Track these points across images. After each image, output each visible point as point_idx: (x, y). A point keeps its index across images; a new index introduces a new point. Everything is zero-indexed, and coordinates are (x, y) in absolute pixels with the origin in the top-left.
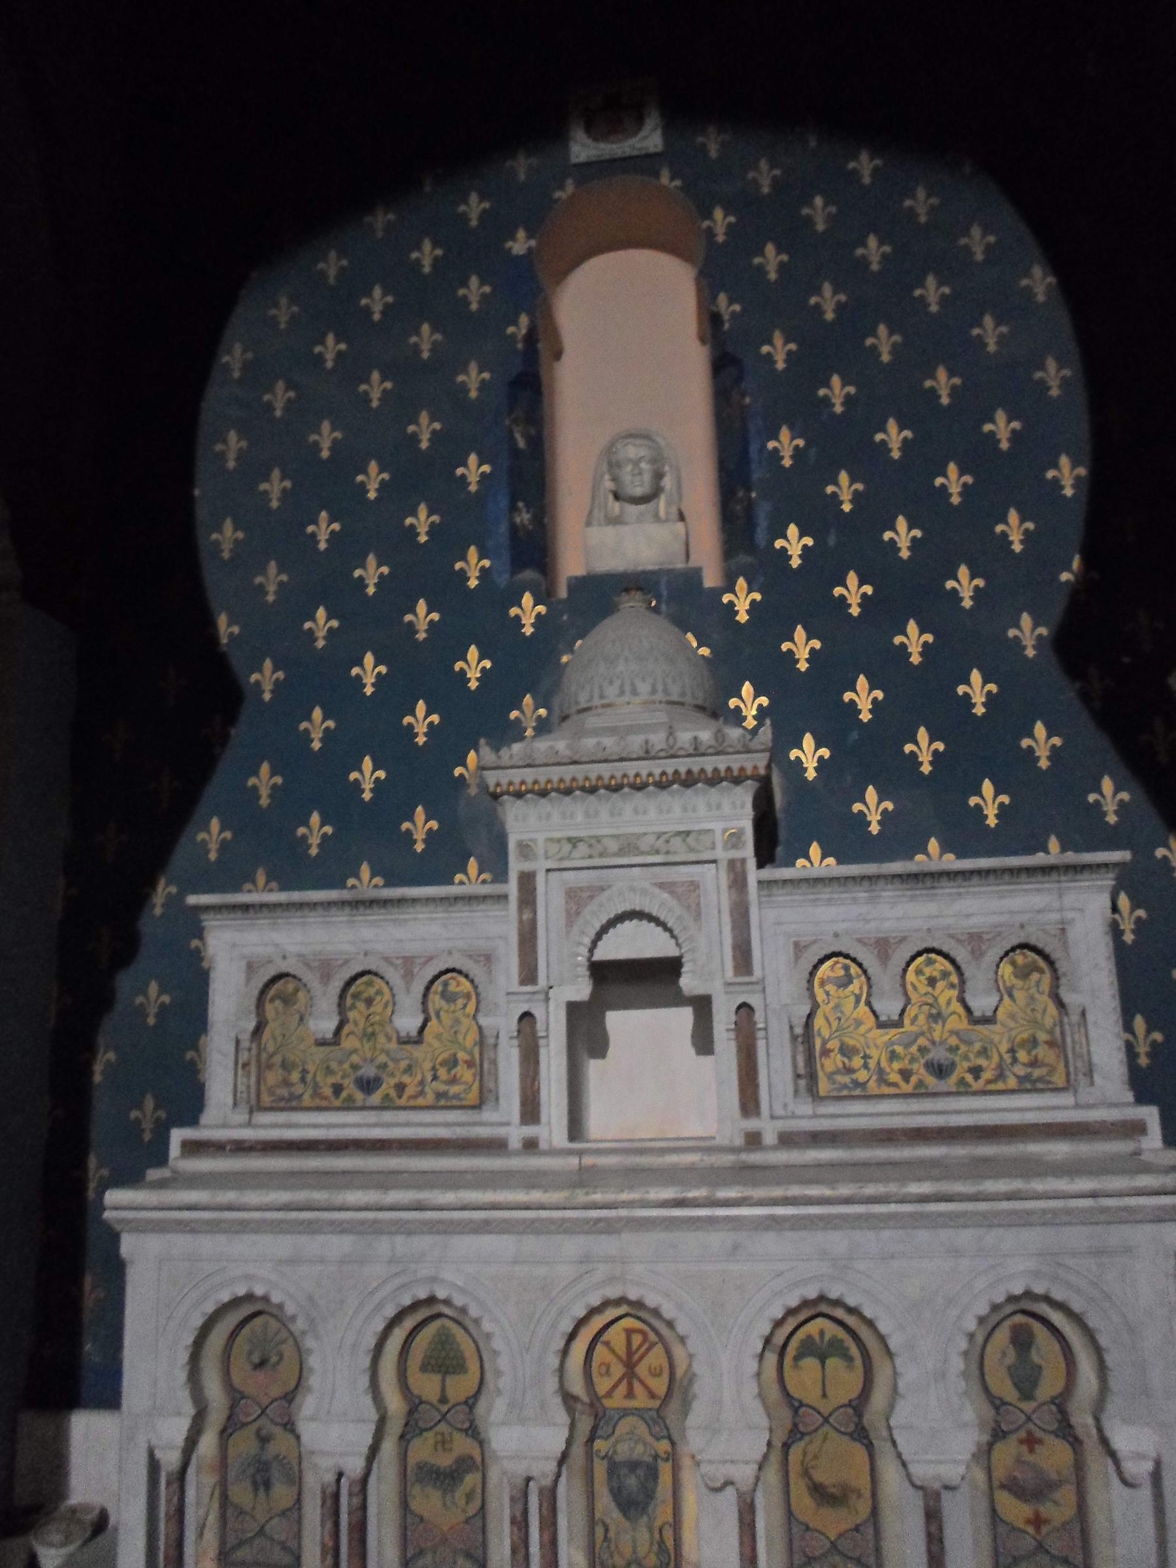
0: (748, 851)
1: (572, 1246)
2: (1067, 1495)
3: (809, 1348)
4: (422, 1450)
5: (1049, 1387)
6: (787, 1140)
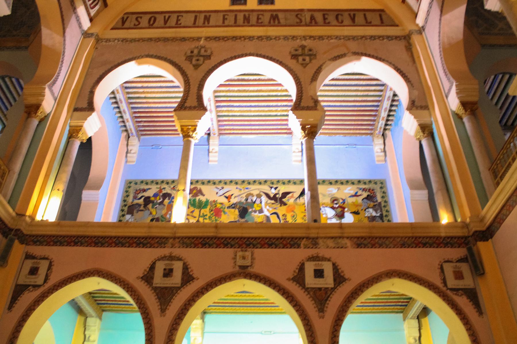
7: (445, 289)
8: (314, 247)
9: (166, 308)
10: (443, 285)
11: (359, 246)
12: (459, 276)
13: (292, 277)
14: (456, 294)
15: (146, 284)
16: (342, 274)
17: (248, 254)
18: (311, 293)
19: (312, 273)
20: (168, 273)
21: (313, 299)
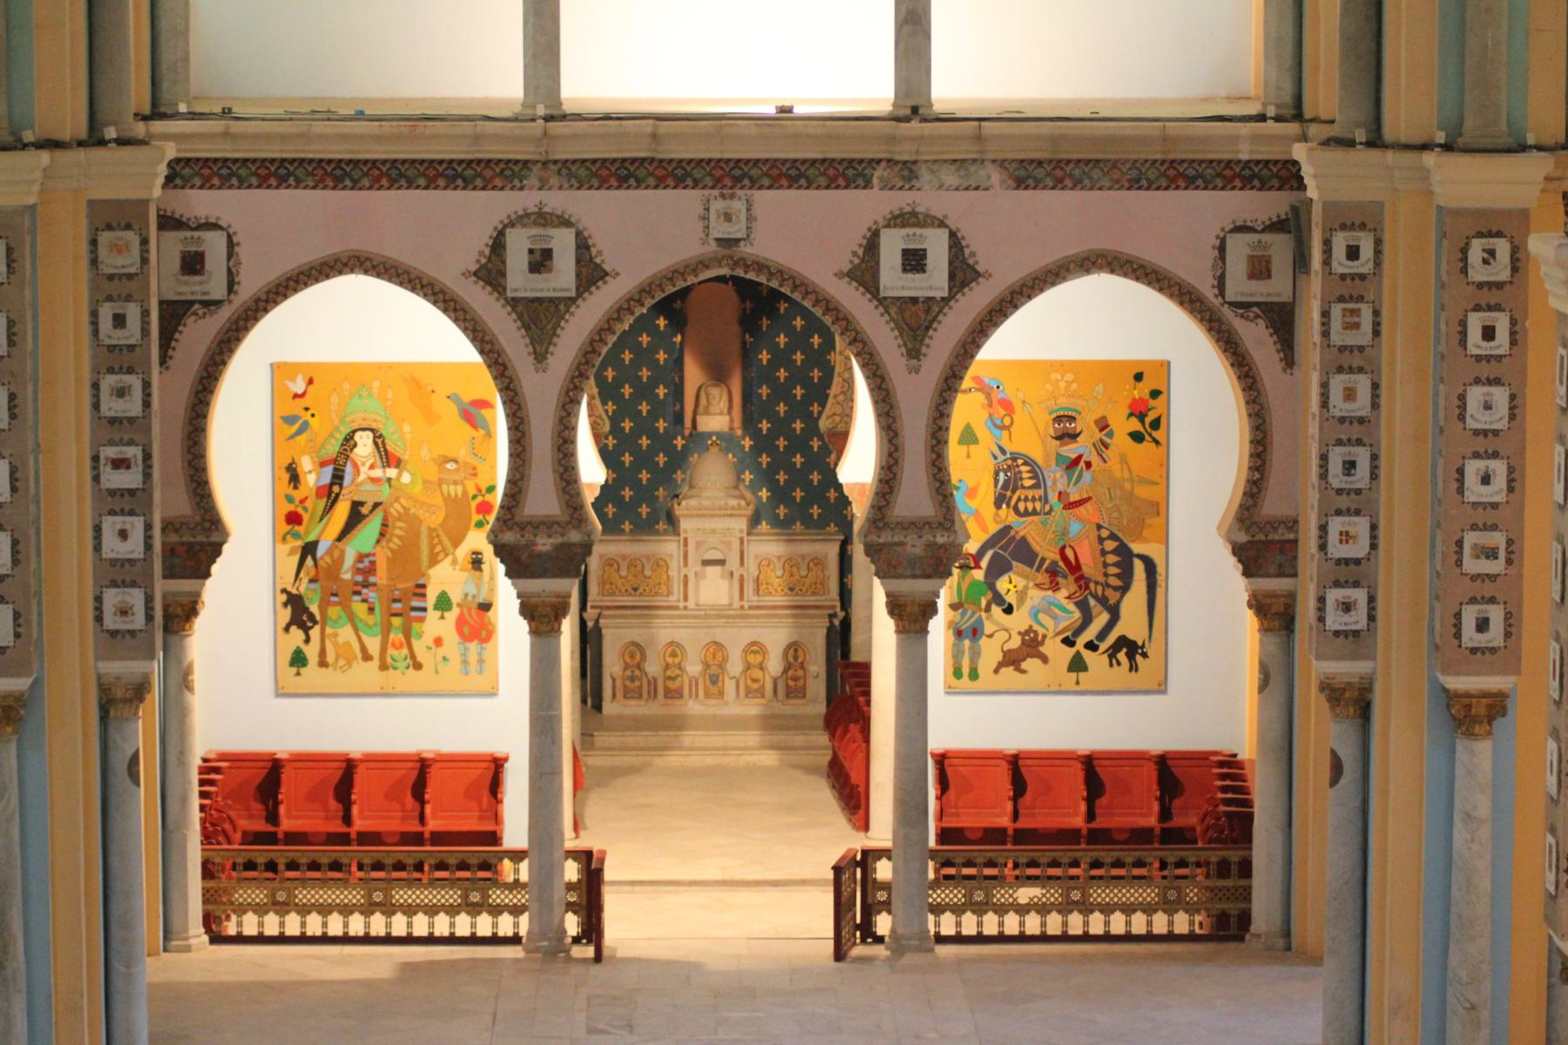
0: (744, 535)
1: (705, 631)
2: (802, 681)
3: (752, 652)
4: (669, 673)
5: (800, 660)
6: (751, 608)
7: (1217, 302)
8: (907, 186)
9: (547, 352)
10: (1216, 291)
11: (1021, 183)
12: (1260, 269)
13: (846, 267)
14: (1242, 316)
15: (489, 289)
16: (971, 262)
17: (738, 206)
18: (893, 311)
19: (897, 259)
20: (541, 261)
21: (898, 327)
